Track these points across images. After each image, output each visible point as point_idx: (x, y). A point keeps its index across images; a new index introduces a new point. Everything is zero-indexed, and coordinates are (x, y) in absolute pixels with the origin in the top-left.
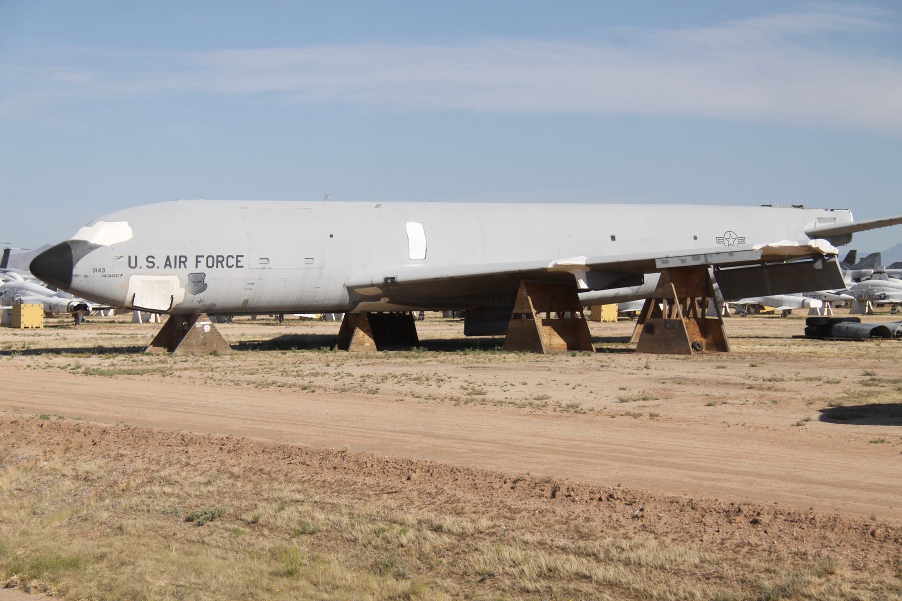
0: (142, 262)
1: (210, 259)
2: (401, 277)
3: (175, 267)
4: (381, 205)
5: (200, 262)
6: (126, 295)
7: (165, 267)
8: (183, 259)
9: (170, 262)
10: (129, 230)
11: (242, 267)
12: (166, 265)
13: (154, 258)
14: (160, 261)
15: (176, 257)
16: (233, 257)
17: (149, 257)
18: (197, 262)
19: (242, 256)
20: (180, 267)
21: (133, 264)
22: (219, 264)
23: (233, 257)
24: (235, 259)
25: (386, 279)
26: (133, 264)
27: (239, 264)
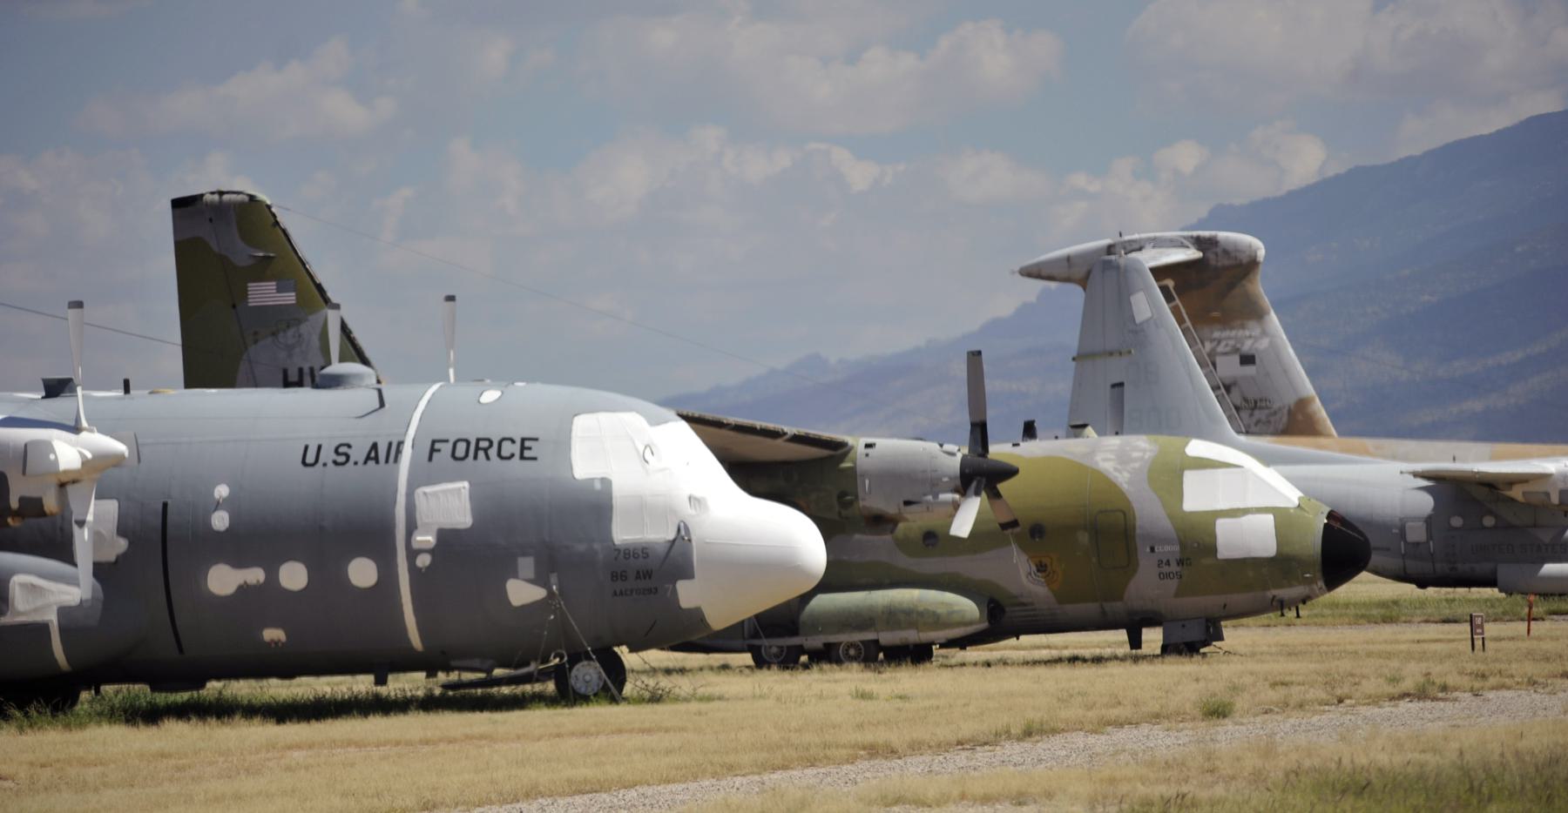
5: (439, 450)
7: (365, 463)
16: (513, 441)
21: (310, 458)
26: (310, 458)
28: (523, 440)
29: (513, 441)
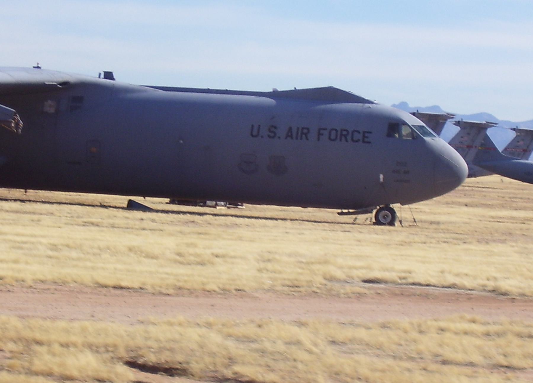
1: (333, 133)
5: (322, 134)
7: (286, 138)
8: (305, 131)
9: (292, 134)
11: (369, 142)
15: (298, 128)
16: (359, 133)
18: (320, 134)
19: (370, 133)
21: (255, 133)
24: (361, 135)
26: (255, 133)
28: (364, 132)
29: (359, 133)
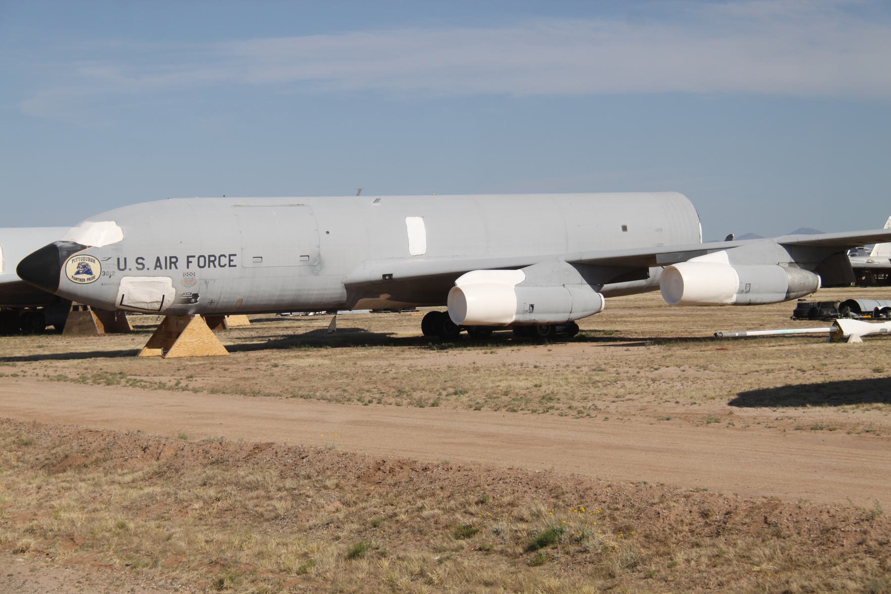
0: (131, 263)
1: (202, 259)
2: (397, 275)
3: (166, 268)
4: (380, 199)
5: (191, 262)
6: (117, 296)
7: (155, 269)
8: (174, 260)
10: (119, 229)
11: (235, 266)
12: (156, 266)
13: (143, 259)
14: (150, 262)
15: (166, 258)
16: (226, 257)
17: (139, 258)
18: (189, 262)
19: (235, 255)
20: (170, 268)
21: (122, 266)
22: (211, 264)
23: (226, 257)
25: (384, 276)
26: (122, 266)
27: (232, 263)
28: (230, 255)
